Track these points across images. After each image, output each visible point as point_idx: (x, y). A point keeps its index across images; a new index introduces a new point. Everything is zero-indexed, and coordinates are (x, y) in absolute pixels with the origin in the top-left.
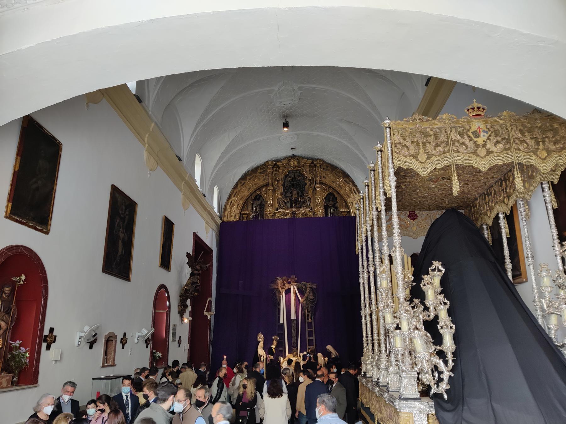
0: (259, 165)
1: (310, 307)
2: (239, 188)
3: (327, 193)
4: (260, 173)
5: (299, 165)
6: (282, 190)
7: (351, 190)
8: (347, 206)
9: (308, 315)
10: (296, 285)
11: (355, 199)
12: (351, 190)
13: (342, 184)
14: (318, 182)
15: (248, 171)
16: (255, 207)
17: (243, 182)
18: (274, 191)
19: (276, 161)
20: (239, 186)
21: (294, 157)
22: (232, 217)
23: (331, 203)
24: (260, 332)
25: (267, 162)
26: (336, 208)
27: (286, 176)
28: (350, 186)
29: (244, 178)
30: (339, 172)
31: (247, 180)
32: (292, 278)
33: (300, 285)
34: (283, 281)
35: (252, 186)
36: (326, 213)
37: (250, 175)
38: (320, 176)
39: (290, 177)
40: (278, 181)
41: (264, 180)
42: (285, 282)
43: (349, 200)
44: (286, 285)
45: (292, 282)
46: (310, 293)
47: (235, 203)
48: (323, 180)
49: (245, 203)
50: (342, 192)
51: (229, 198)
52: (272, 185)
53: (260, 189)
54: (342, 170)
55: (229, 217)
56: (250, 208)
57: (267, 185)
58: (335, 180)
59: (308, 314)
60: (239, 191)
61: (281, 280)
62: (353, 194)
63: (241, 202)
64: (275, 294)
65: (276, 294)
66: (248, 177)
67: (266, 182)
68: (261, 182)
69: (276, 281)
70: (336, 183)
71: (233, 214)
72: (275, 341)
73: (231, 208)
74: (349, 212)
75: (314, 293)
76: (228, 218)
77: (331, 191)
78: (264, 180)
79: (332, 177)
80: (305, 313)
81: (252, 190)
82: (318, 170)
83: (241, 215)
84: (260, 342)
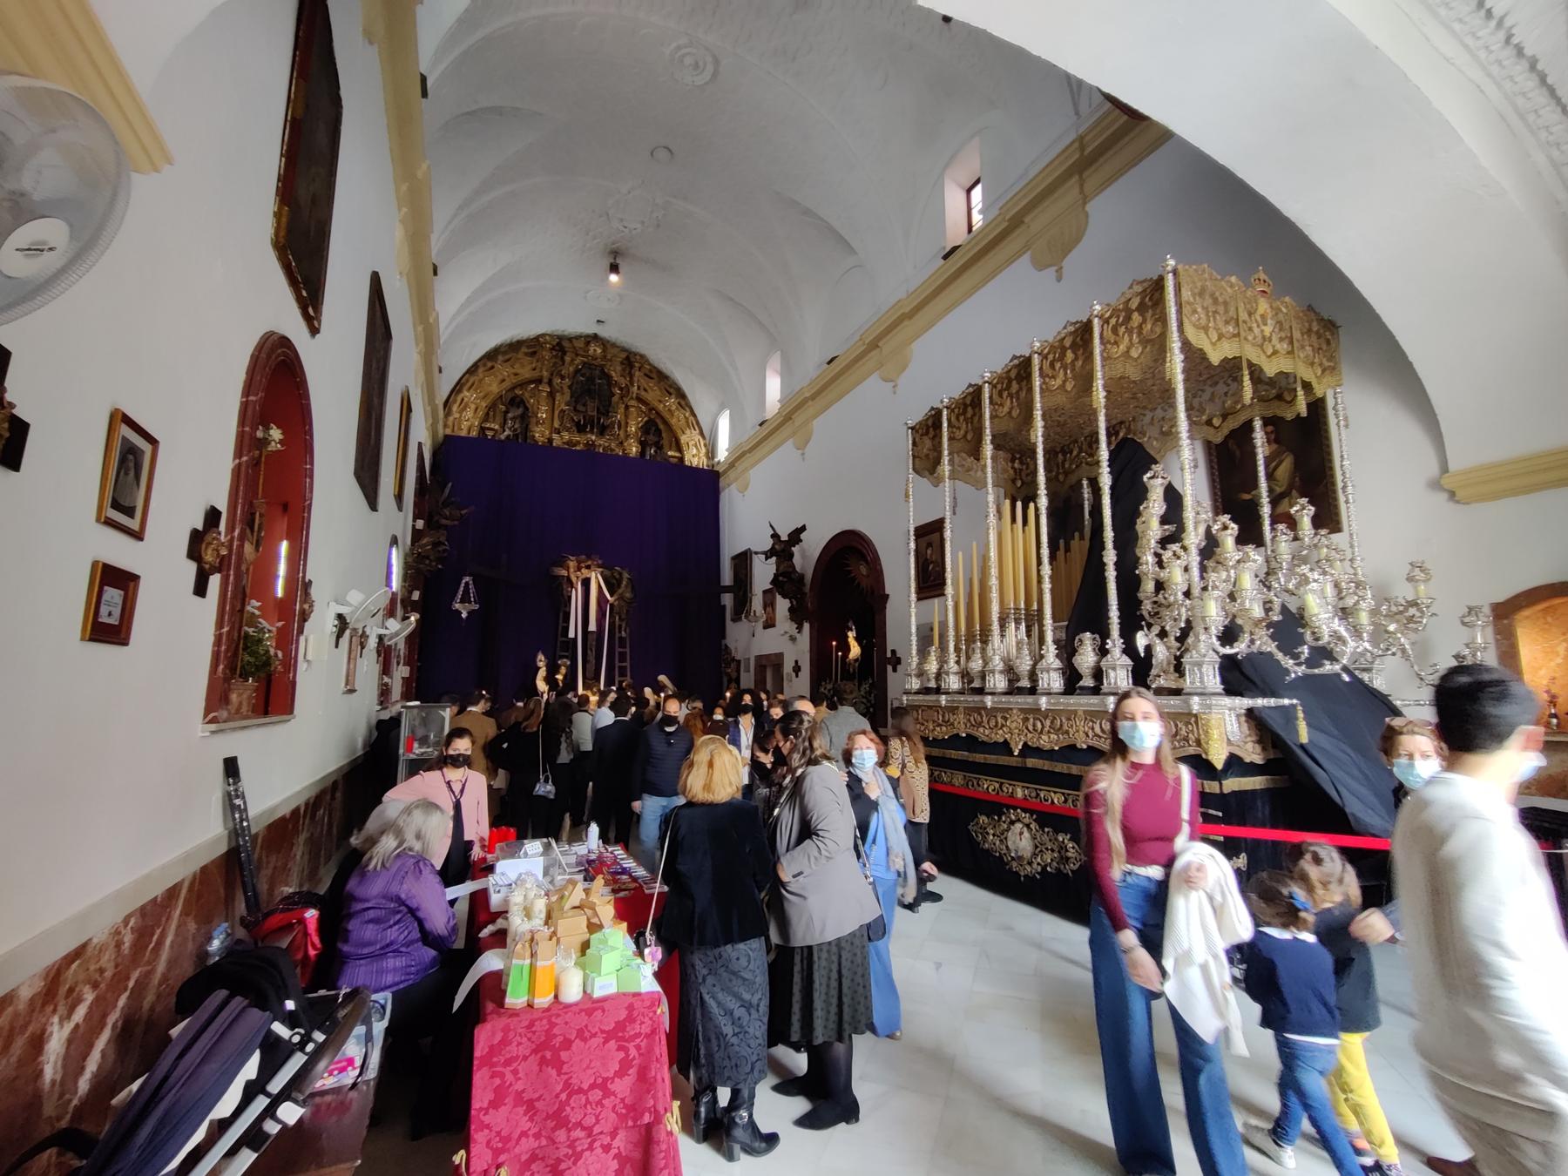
0: (525, 338)
2: (481, 376)
3: (646, 419)
4: (526, 354)
5: (605, 357)
6: (567, 397)
7: (687, 422)
8: (680, 450)
9: (620, 626)
10: (602, 574)
12: (687, 422)
14: (634, 395)
15: (501, 345)
16: (511, 419)
18: (552, 395)
20: (481, 370)
21: (595, 337)
23: (652, 438)
25: (543, 335)
26: (659, 447)
27: (577, 371)
28: (687, 414)
29: (492, 355)
30: (671, 386)
33: (607, 573)
34: (579, 562)
35: (509, 376)
36: (643, 453)
37: (505, 353)
38: (639, 388)
39: (582, 375)
40: (563, 378)
41: (534, 369)
43: (683, 439)
45: (592, 568)
48: (643, 393)
49: (492, 407)
50: (673, 421)
52: (550, 383)
53: (523, 385)
56: (499, 418)
57: (539, 381)
60: (481, 381)
64: (561, 584)
66: (500, 358)
67: (536, 374)
68: (526, 373)
71: (465, 425)
73: (461, 412)
74: (682, 459)
76: (453, 431)
77: (652, 417)
78: (534, 369)
79: (658, 393)
80: (614, 622)
81: (507, 384)
83: (482, 429)
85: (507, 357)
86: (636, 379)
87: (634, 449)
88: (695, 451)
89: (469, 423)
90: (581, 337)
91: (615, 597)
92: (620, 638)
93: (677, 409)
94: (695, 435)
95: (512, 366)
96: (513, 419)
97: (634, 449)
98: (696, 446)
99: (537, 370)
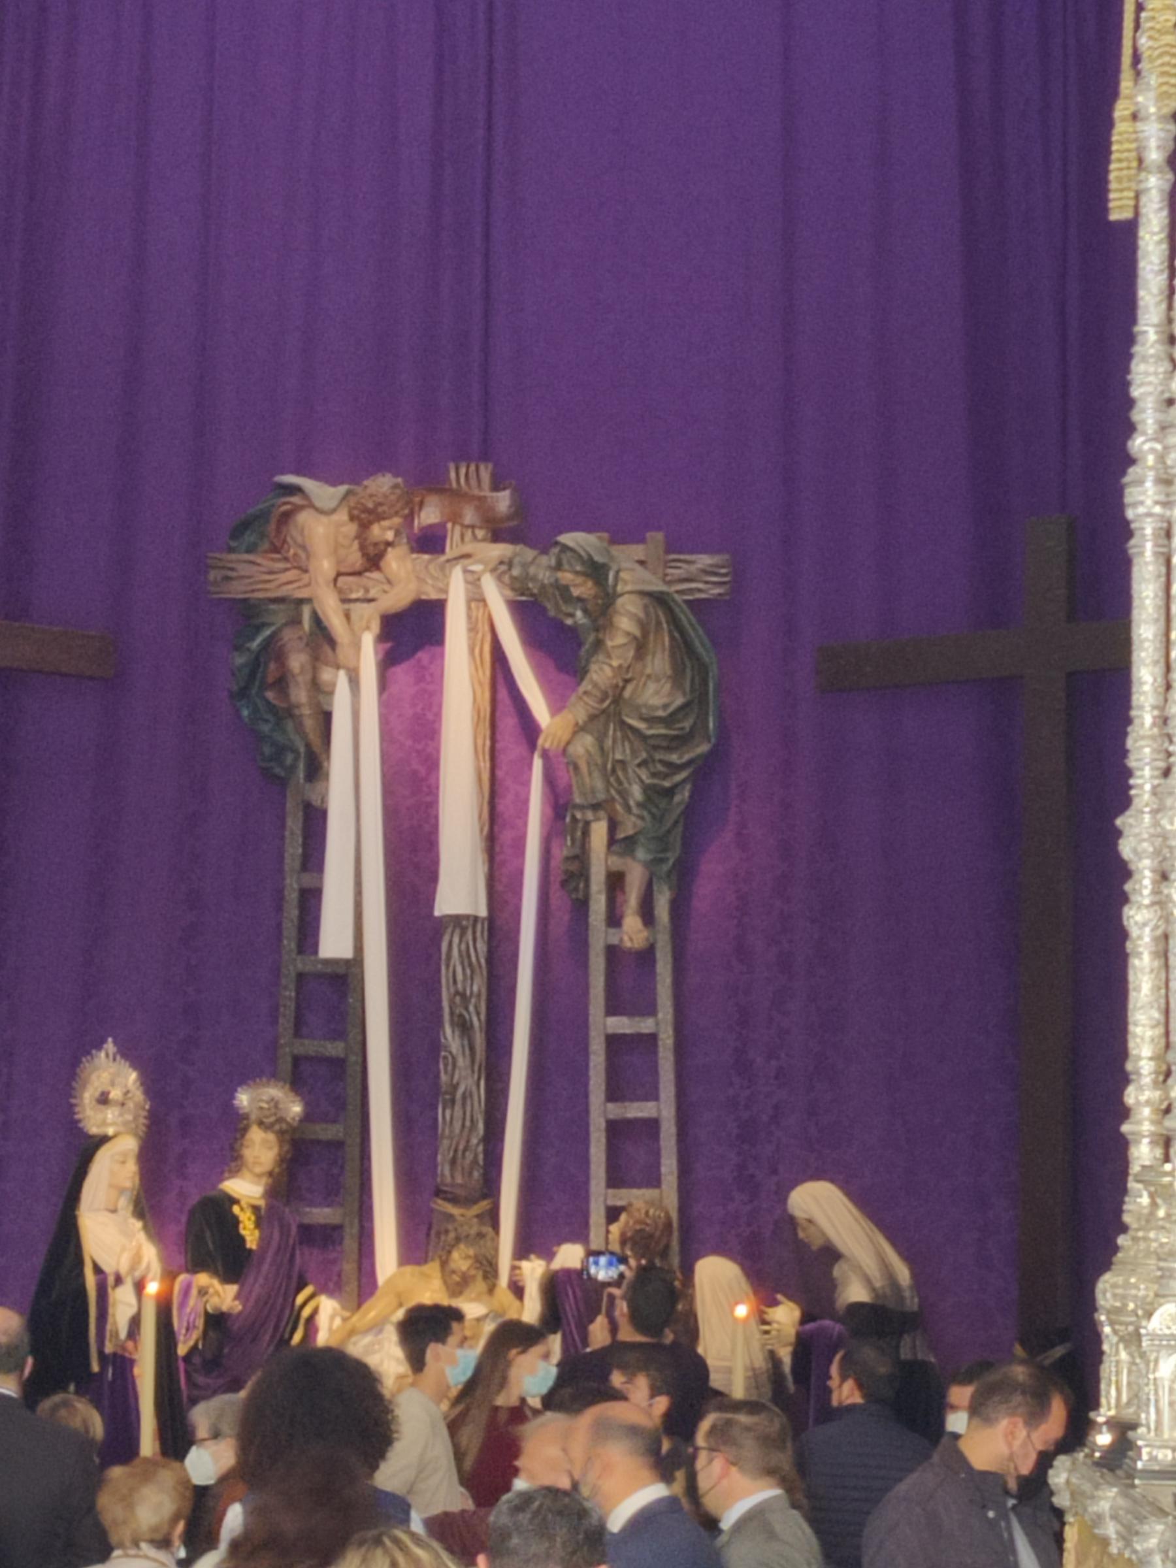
1: (636, 792)
9: (616, 881)
10: (502, 568)
24: (110, 1046)
32: (458, 495)
33: (541, 569)
34: (364, 518)
42: (382, 531)
44: (398, 562)
45: (454, 534)
46: (641, 647)
59: (616, 863)
61: (342, 516)
64: (273, 651)
65: (281, 657)
69: (287, 517)
72: (256, 1135)
75: (683, 650)
80: (581, 858)
84: (104, 1140)
91: (578, 711)
92: (613, 952)
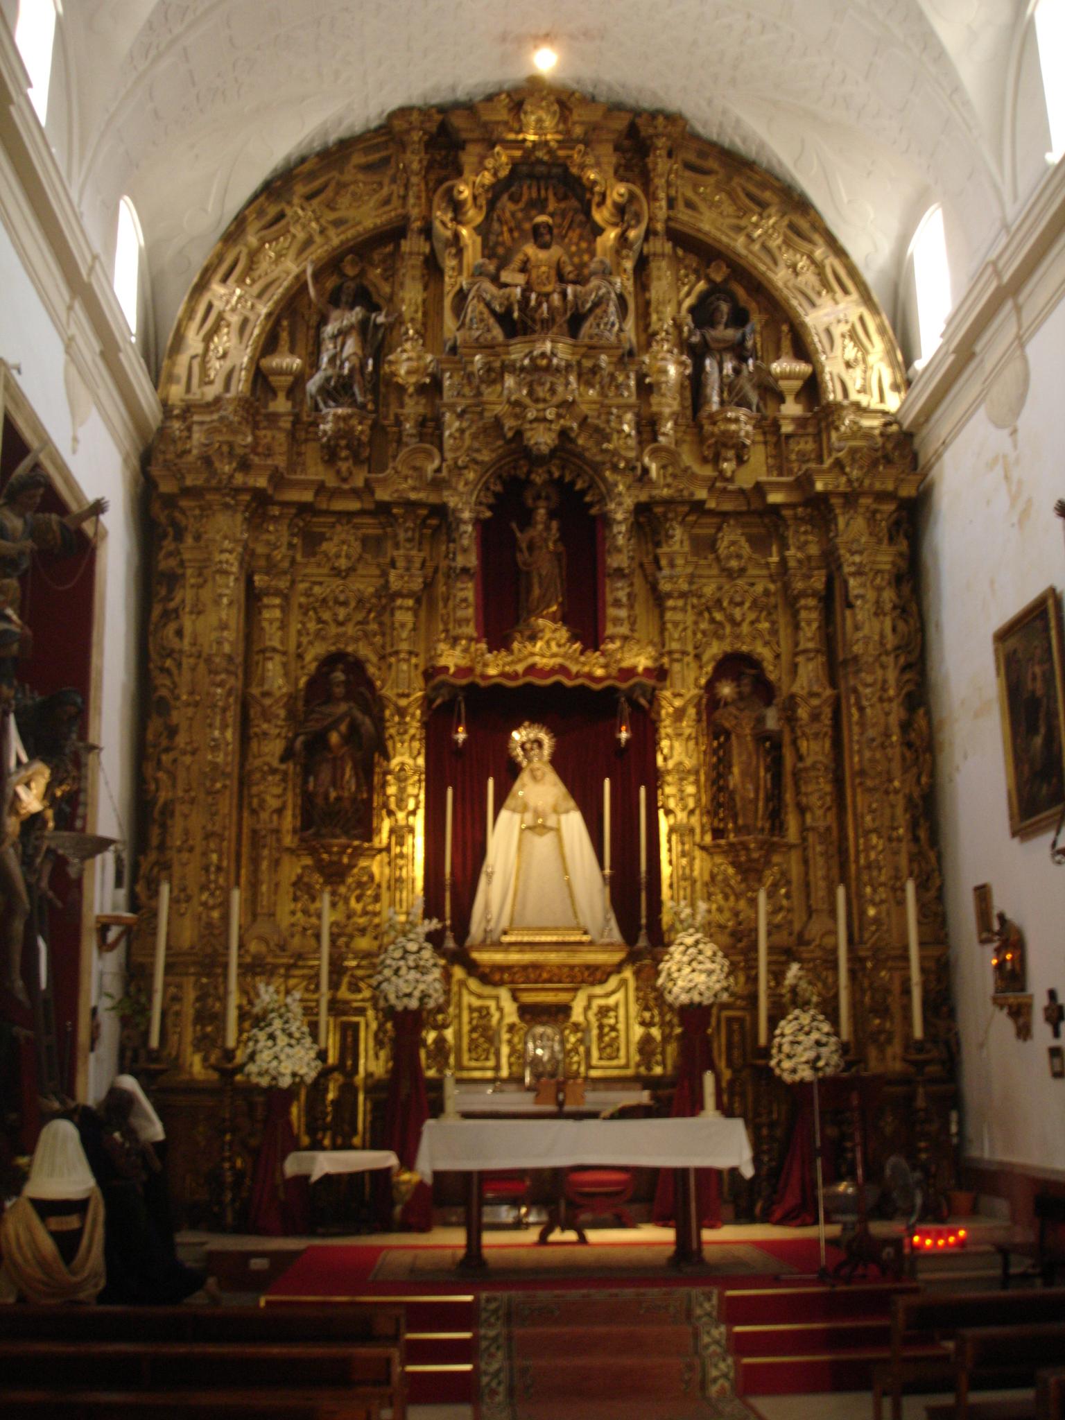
0: (358, 129)
2: (252, 240)
4: (367, 168)
8: (802, 350)
11: (841, 316)
12: (821, 273)
13: (776, 242)
14: (660, 227)
15: (303, 160)
17: (272, 211)
19: (442, 109)
22: (211, 383)
25: (403, 112)
28: (819, 253)
30: (764, 186)
31: (296, 200)
35: (322, 231)
38: (671, 203)
47: (228, 316)
48: (683, 214)
50: (780, 277)
51: (201, 287)
52: (427, 232)
54: (777, 179)
55: (195, 381)
58: (743, 223)
60: (253, 256)
62: (830, 290)
63: (263, 310)
66: (301, 189)
70: (749, 237)
78: (387, 202)
79: (729, 208)
81: (319, 251)
82: (661, 164)
83: (260, 378)
85: (317, 184)
86: (660, 182)
87: (672, 370)
88: (851, 352)
89: (228, 364)
90: (498, 94)
93: (787, 242)
94: (848, 309)
95: (331, 206)
96: (343, 333)
97: (672, 370)
98: (853, 335)
99: (396, 202)
